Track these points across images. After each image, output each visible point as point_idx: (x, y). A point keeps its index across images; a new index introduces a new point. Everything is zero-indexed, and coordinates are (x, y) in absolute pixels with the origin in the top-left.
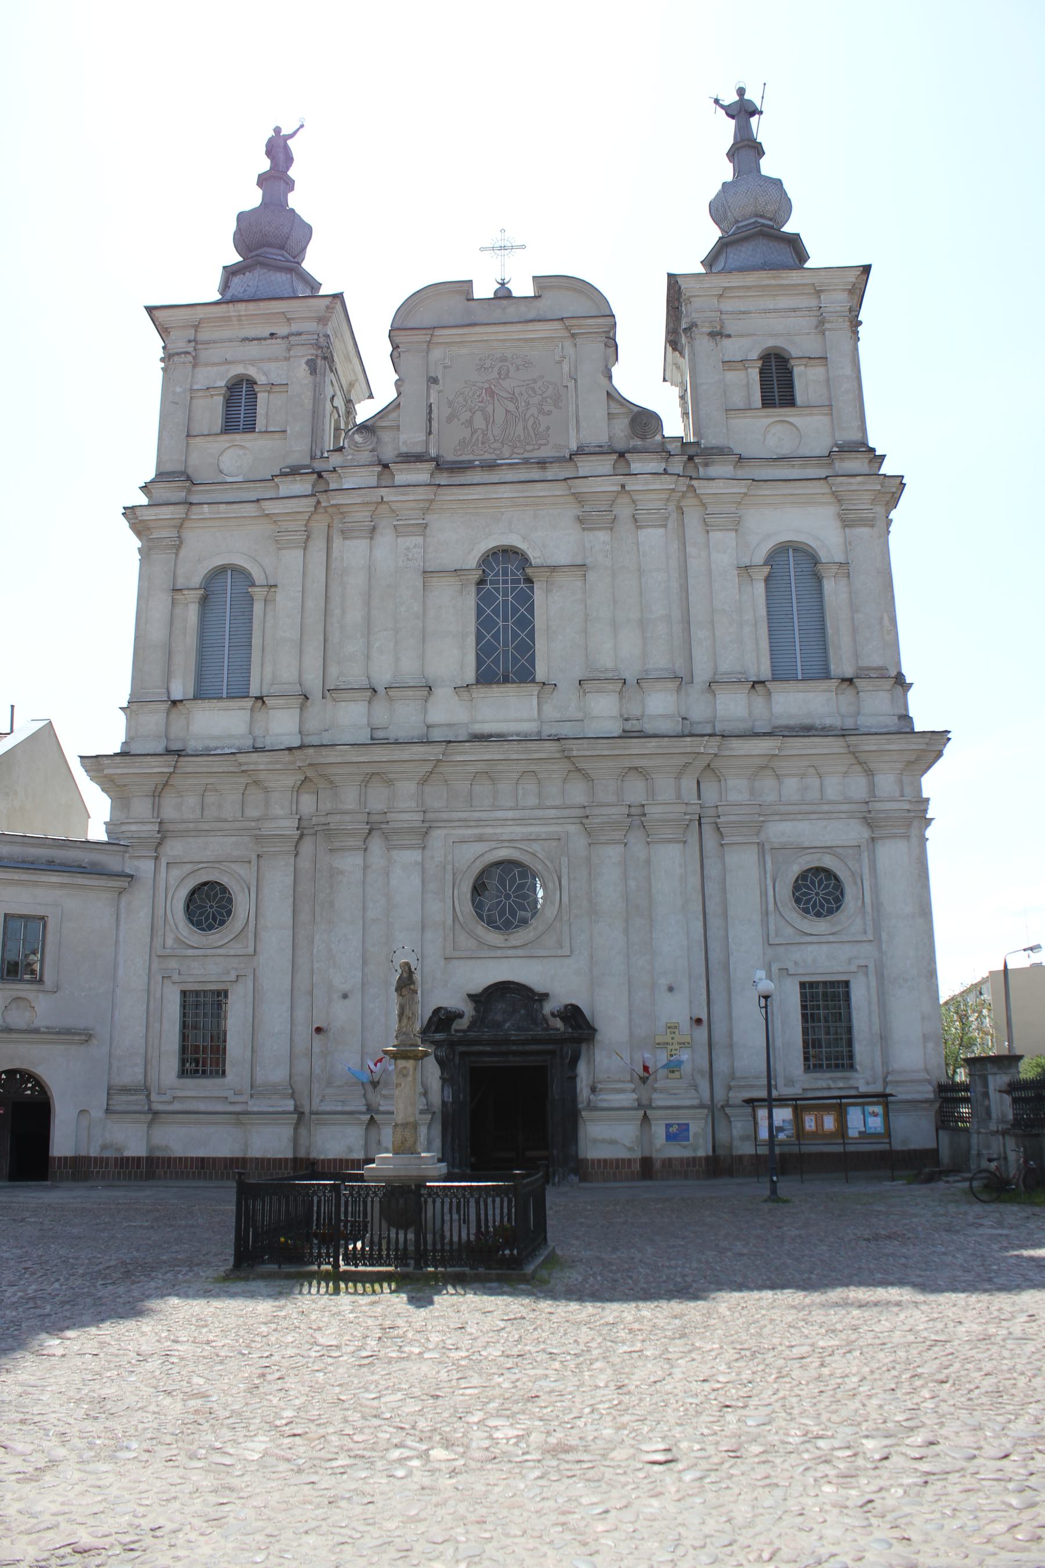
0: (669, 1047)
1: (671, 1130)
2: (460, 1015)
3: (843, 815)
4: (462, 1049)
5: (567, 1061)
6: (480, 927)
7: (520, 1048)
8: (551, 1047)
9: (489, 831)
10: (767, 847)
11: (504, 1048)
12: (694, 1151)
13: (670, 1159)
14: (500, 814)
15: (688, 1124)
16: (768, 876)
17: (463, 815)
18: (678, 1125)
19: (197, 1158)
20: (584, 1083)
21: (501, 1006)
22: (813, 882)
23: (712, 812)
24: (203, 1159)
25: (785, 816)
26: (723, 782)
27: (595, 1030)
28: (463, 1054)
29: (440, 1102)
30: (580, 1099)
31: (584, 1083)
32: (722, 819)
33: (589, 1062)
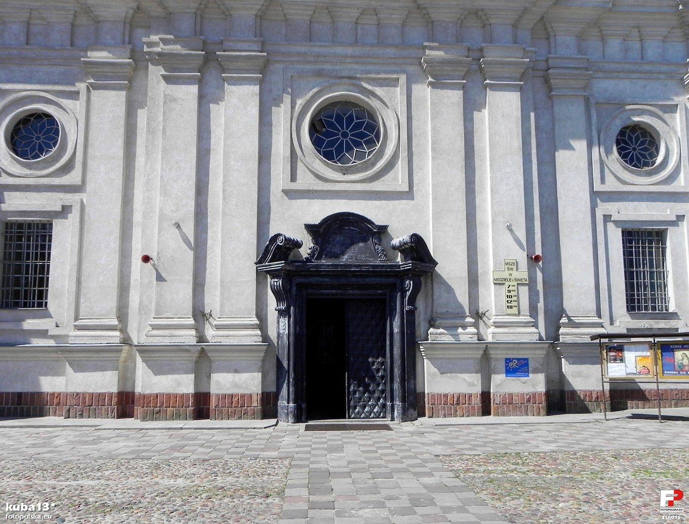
0: (507, 283)
1: (510, 364)
2: (298, 245)
3: (662, 76)
4: (299, 280)
5: (408, 293)
6: (317, 161)
7: (361, 281)
8: (391, 280)
9: (328, 67)
10: (592, 101)
11: (343, 281)
12: (533, 386)
13: (511, 395)
14: (339, 50)
15: (527, 359)
16: (594, 128)
17: (303, 49)
18: (518, 359)
19: (13, 393)
20: (422, 317)
21: (339, 238)
22: (630, 138)
23: (542, 65)
24: (20, 395)
25: (610, 74)
26: (552, 39)
27: (435, 263)
28: (298, 285)
29: (276, 335)
30: (417, 333)
31: (422, 317)
32: (551, 71)
33: (426, 296)
